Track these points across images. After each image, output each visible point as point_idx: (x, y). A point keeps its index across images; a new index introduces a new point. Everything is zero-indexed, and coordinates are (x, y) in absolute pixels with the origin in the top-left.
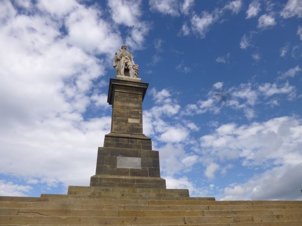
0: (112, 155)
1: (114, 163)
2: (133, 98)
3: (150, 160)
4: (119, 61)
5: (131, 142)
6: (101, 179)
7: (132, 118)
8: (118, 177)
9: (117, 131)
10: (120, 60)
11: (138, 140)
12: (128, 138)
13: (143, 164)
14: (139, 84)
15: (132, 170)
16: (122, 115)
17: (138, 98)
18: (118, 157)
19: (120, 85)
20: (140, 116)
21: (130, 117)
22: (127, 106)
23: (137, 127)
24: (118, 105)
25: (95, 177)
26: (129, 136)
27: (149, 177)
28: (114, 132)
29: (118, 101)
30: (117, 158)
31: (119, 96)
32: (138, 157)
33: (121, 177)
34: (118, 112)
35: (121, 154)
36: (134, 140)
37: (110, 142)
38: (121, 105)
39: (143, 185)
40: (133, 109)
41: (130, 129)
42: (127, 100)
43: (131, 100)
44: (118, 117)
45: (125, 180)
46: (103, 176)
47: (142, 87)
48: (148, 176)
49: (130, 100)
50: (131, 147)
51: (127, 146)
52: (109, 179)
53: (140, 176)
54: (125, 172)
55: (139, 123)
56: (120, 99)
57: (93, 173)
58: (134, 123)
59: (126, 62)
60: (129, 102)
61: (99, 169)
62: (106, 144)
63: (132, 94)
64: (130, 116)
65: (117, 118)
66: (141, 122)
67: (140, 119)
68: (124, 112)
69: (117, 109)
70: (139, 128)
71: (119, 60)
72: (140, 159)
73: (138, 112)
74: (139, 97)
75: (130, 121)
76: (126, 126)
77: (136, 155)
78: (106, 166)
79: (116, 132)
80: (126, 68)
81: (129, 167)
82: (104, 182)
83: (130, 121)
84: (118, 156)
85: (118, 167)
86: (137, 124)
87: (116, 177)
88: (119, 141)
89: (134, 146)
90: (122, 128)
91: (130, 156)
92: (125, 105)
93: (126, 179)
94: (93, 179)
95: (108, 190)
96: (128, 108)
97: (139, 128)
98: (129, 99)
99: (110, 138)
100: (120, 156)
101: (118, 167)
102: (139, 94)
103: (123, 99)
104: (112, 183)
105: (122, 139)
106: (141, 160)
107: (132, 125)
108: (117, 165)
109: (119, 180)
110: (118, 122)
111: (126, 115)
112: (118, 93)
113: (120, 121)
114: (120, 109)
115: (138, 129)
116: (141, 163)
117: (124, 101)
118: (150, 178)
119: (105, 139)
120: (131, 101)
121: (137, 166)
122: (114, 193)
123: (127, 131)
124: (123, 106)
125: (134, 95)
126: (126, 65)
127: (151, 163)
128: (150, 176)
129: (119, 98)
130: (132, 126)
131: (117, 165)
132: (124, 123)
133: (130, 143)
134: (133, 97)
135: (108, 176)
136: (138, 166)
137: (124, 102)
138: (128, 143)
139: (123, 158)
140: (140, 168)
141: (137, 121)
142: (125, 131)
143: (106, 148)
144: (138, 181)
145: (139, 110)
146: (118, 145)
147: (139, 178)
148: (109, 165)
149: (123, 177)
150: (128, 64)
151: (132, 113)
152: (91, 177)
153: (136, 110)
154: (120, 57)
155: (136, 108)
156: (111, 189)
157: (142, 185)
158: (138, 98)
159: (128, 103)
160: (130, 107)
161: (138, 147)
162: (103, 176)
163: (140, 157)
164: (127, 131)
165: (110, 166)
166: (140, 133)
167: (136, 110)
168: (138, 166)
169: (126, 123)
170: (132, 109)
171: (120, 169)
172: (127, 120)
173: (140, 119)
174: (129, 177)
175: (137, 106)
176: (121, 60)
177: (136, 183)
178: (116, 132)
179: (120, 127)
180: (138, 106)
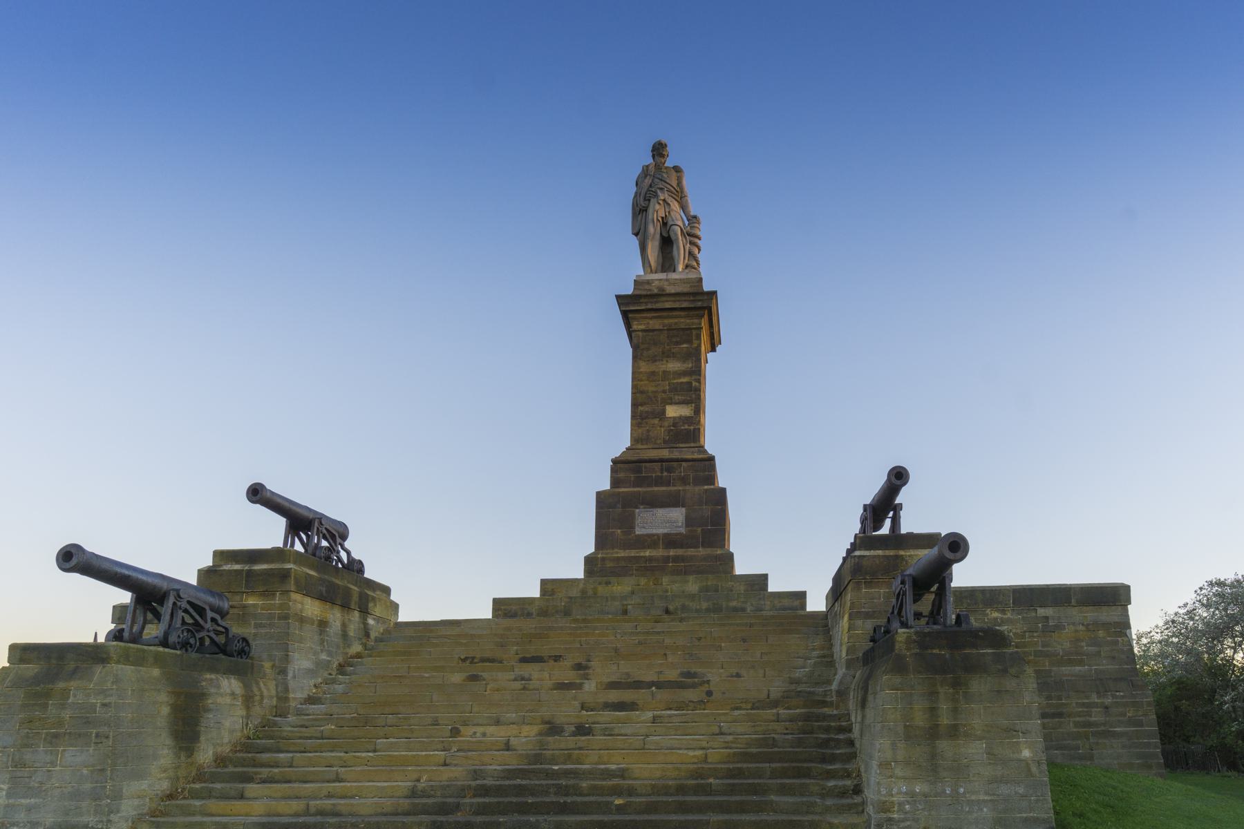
1: (628, 523)
2: (677, 343)
3: (706, 511)
4: (644, 213)
5: (669, 470)
6: (603, 559)
8: (637, 553)
9: (642, 444)
10: (646, 211)
11: (684, 464)
12: (661, 461)
13: (689, 521)
15: (666, 535)
18: (637, 510)
20: (694, 396)
21: (669, 401)
22: (664, 372)
23: (686, 427)
24: (641, 372)
25: (593, 556)
26: (665, 454)
29: (640, 359)
30: (634, 512)
31: (642, 343)
33: (642, 554)
35: (642, 504)
36: (675, 464)
37: (621, 475)
38: (648, 370)
39: (685, 566)
41: (671, 433)
42: (663, 353)
43: (673, 351)
45: (650, 559)
46: (607, 554)
48: (699, 547)
50: (668, 484)
51: (659, 482)
52: (618, 559)
53: (682, 547)
58: (680, 417)
59: (664, 216)
61: (602, 538)
62: (615, 482)
64: (671, 399)
65: (640, 407)
66: (698, 409)
67: (693, 405)
68: (654, 389)
69: (639, 383)
71: (643, 211)
72: (684, 509)
74: (694, 338)
75: (672, 411)
76: (661, 427)
77: (673, 501)
78: (614, 532)
80: (665, 235)
81: (661, 531)
82: (609, 564)
83: (672, 411)
84: (637, 508)
85: (637, 533)
87: (633, 553)
88: (639, 471)
89: (674, 479)
90: (651, 433)
92: (657, 370)
93: (652, 556)
94: (589, 561)
95: (610, 583)
97: (692, 428)
98: (667, 347)
99: (622, 466)
100: (642, 507)
104: (621, 570)
105: (648, 464)
106: (686, 513)
107: (676, 421)
108: (637, 529)
109: (637, 559)
110: (642, 419)
111: (660, 396)
112: (640, 333)
113: (647, 418)
114: (647, 382)
115: (688, 431)
116: (686, 519)
117: (654, 360)
118: (702, 551)
119: (613, 470)
120: (673, 353)
121: (676, 527)
122: (619, 587)
123: (665, 442)
124: (653, 373)
126: (665, 224)
127: (708, 516)
129: (643, 349)
130: (675, 425)
131: (637, 527)
132: (656, 421)
133: (665, 474)
134: (678, 339)
135: (617, 553)
136: (680, 527)
137: (655, 361)
138: (662, 473)
140: (683, 530)
141: (685, 411)
142: (659, 442)
144: (676, 559)
145: (694, 377)
146: (639, 482)
147: (680, 552)
148: (620, 529)
149: (647, 553)
151: (675, 389)
152: (585, 557)
154: (645, 200)
156: (613, 579)
157: (683, 568)
159: (665, 362)
160: (670, 372)
161: (684, 480)
162: (607, 554)
163: (683, 507)
164: (665, 442)
165: (622, 532)
166: (694, 442)
168: (680, 527)
169: (660, 420)
170: (675, 379)
171: (642, 535)
172: (664, 412)
173: (693, 405)
174: (659, 552)
177: (671, 564)
179: (648, 431)
180: (690, 365)
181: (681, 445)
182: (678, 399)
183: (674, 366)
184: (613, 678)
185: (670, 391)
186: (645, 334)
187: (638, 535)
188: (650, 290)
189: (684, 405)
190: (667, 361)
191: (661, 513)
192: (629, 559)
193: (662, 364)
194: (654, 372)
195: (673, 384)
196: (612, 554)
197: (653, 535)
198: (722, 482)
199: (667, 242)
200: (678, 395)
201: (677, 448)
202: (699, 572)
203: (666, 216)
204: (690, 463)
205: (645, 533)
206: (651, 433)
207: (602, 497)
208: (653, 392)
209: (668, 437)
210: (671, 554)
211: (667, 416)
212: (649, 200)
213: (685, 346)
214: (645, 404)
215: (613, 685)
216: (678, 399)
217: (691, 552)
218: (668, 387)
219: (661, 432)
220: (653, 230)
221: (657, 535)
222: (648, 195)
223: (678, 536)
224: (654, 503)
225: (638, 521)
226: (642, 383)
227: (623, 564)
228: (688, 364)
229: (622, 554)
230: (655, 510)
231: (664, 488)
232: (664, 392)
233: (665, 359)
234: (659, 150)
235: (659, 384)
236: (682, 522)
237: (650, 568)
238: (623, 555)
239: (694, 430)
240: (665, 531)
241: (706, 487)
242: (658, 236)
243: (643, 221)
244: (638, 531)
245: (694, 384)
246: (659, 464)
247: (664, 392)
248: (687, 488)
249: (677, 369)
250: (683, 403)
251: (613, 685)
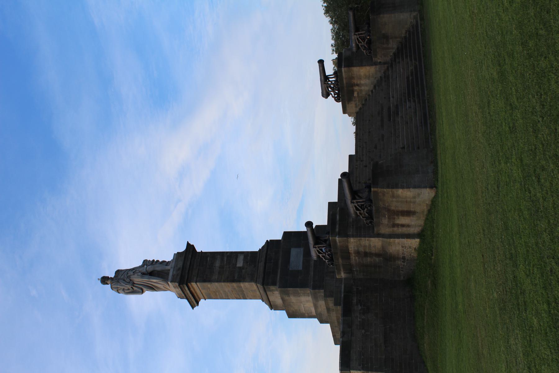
7: (236, 262)
15: (304, 256)
18: (290, 269)
19: (188, 276)
23: (249, 257)
33: (313, 264)
59: (140, 273)
62: (274, 284)
67: (239, 254)
70: (250, 255)
75: (240, 264)
83: (240, 264)
85: (301, 269)
91: (290, 259)
126: (143, 274)
132: (244, 271)
140: (302, 249)
143: (278, 284)
150: (145, 271)
153: (225, 258)
167: (225, 258)
172: (240, 268)
176: (135, 282)
180: (219, 256)
183: (217, 264)
189: (238, 259)
190: (215, 266)
191: (292, 259)
197: (303, 262)
198: (279, 236)
199: (152, 274)
211: (242, 266)
212: (131, 280)
220: (145, 280)
222: (127, 281)
224: (287, 261)
234: (104, 280)
244: (301, 268)
245: (228, 254)
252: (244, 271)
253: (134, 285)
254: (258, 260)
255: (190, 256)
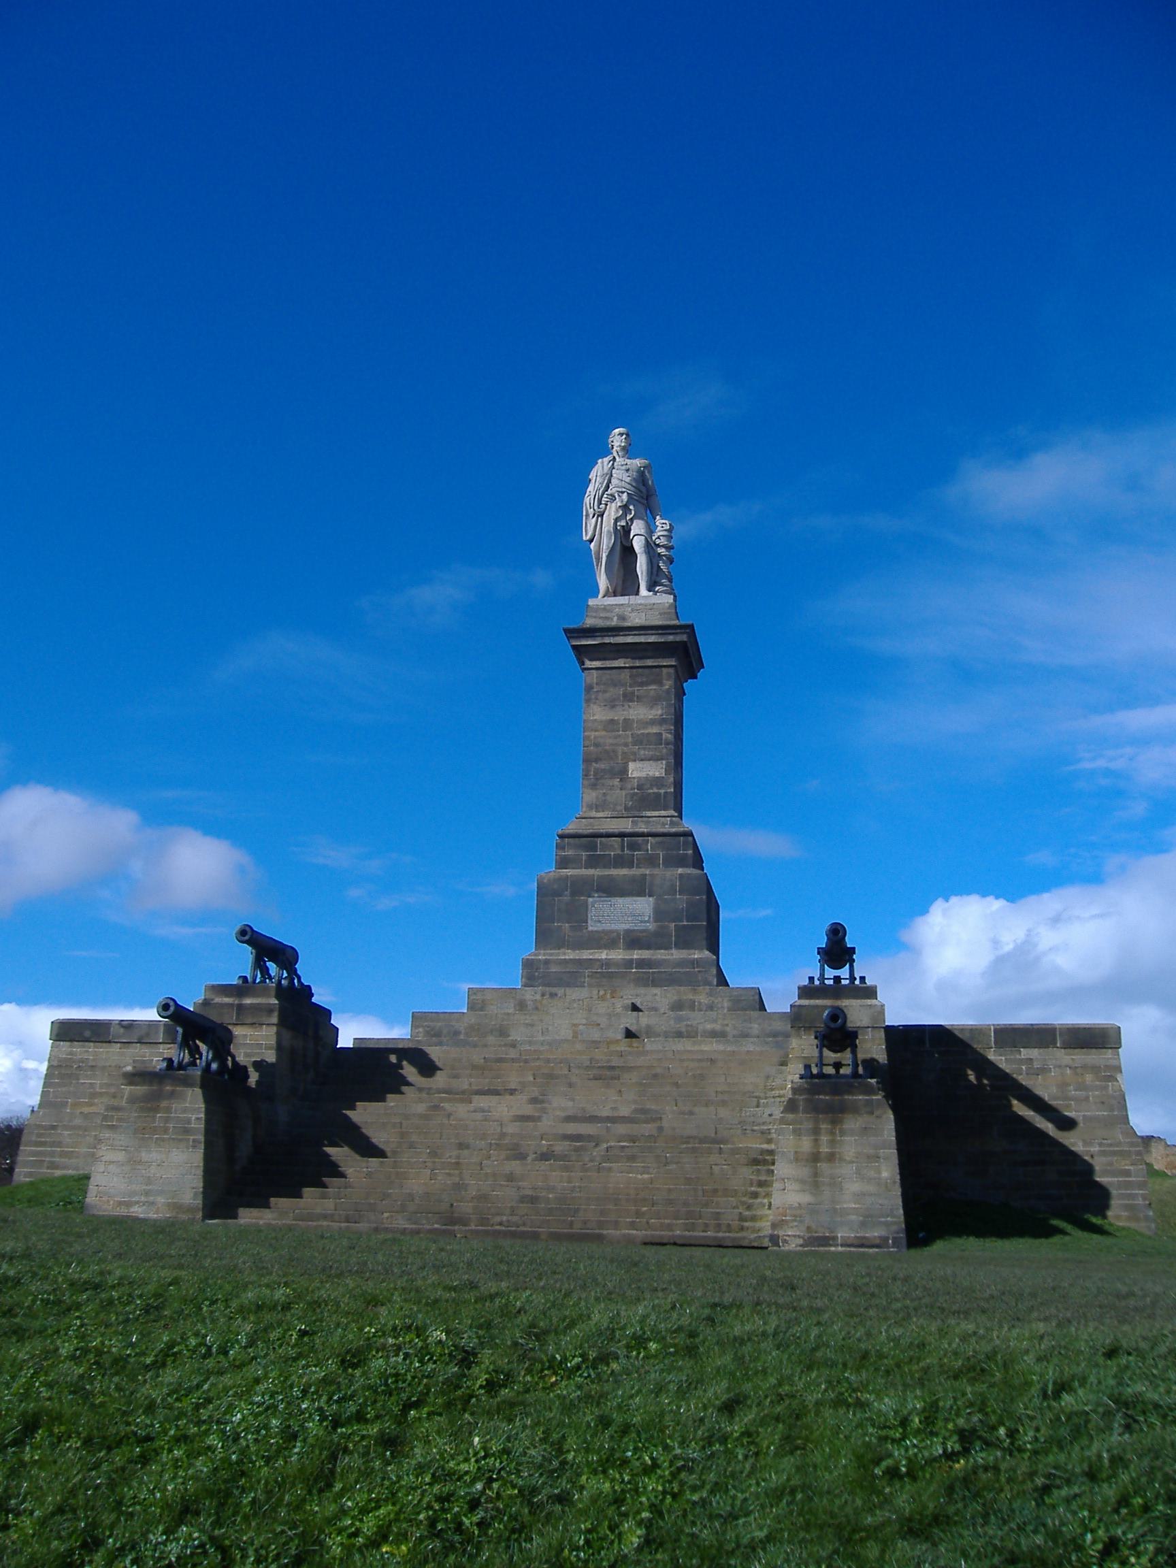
0: (573, 894)
1: (578, 916)
2: (642, 684)
6: (547, 962)
8: (591, 954)
10: (602, 516)
12: (622, 835)
13: (659, 915)
14: (660, 632)
15: (627, 932)
16: (609, 755)
17: (660, 683)
18: (590, 900)
20: (665, 751)
26: (626, 826)
27: (674, 951)
28: (587, 815)
29: (595, 703)
30: (586, 904)
32: (645, 896)
33: (597, 956)
34: (596, 745)
35: (597, 891)
37: (570, 853)
38: (604, 718)
40: (644, 728)
42: (625, 695)
44: (597, 760)
45: (607, 963)
46: (551, 955)
47: (671, 638)
48: (671, 948)
49: (633, 693)
50: (630, 865)
51: (620, 862)
53: (648, 947)
54: (609, 940)
55: (664, 775)
56: (600, 696)
57: (527, 947)
58: (647, 778)
60: (632, 701)
61: (544, 936)
62: (563, 863)
63: (640, 670)
65: (594, 764)
67: (664, 762)
72: (651, 899)
73: (660, 734)
74: (664, 676)
76: (621, 789)
77: (639, 888)
79: (593, 814)
81: (623, 927)
84: (590, 897)
85: (590, 928)
86: (657, 782)
87: (586, 955)
90: (608, 798)
91: (623, 894)
96: (627, 724)
97: (662, 791)
99: (571, 840)
101: (590, 928)
102: (665, 666)
103: (614, 692)
104: (571, 976)
110: (597, 779)
111: (620, 750)
114: (604, 733)
117: (612, 704)
118: (676, 954)
121: (641, 922)
124: (612, 721)
125: (647, 671)
126: (626, 530)
128: (677, 946)
129: (597, 691)
131: (589, 921)
132: (616, 782)
134: (644, 679)
135: (565, 954)
136: (645, 922)
137: (613, 707)
138: (623, 851)
139: (607, 901)
140: (651, 926)
142: (619, 808)
144: (641, 963)
145: (664, 727)
146: (593, 862)
147: (645, 954)
148: (568, 923)
149: (603, 955)
151: (639, 741)
153: (655, 730)
154: (600, 503)
155: (653, 722)
158: (660, 683)
161: (651, 861)
162: (551, 955)
163: (650, 896)
164: (626, 809)
168: (645, 922)
172: (625, 771)
173: (664, 762)
174: (618, 955)
175: (657, 712)
178: (593, 814)
180: (660, 712)
181: (649, 814)
182: (645, 755)
184: (570, 1113)
185: (634, 744)
186: (600, 672)
187: (592, 931)
188: (607, 618)
190: (629, 706)
191: (620, 902)
192: (579, 962)
193: (624, 710)
194: (612, 720)
195: (638, 735)
196: (558, 954)
197: (611, 931)
200: (644, 749)
201: (642, 817)
202: (670, 980)
203: (627, 523)
204: (658, 839)
205: (600, 929)
206: (608, 798)
207: (545, 881)
208: (612, 744)
209: (631, 803)
210: (635, 957)
212: (607, 505)
213: (653, 687)
214: (601, 760)
215: (569, 1119)
216: (645, 755)
217: (661, 955)
218: (630, 740)
219: (619, 795)
221: (617, 931)
222: (605, 496)
223: (644, 934)
224: (610, 889)
225: (592, 914)
226: (597, 733)
227: (570, 968)
228: (657, 710)
229: (570, 955)
230: (614, 900)
231: (624, 872)
232: (626, 745)
233: (626, 704)
235: (620, 736)
236: (650, 917)
237: (607, 975)
238: (571, 957)
239: (666, 793)
240: (626, 927)
241: (680, 871)
242: (618, 548)
243: (599, 523)
246: (619, 839)
247: (626, 745)
248: (656, 871)
249: (642, 717)
250: (649, 760)
251: (569, 1119)
252: (616, 782)
253: (600, 518)
254: (637, 813)
255: (652, 639)
